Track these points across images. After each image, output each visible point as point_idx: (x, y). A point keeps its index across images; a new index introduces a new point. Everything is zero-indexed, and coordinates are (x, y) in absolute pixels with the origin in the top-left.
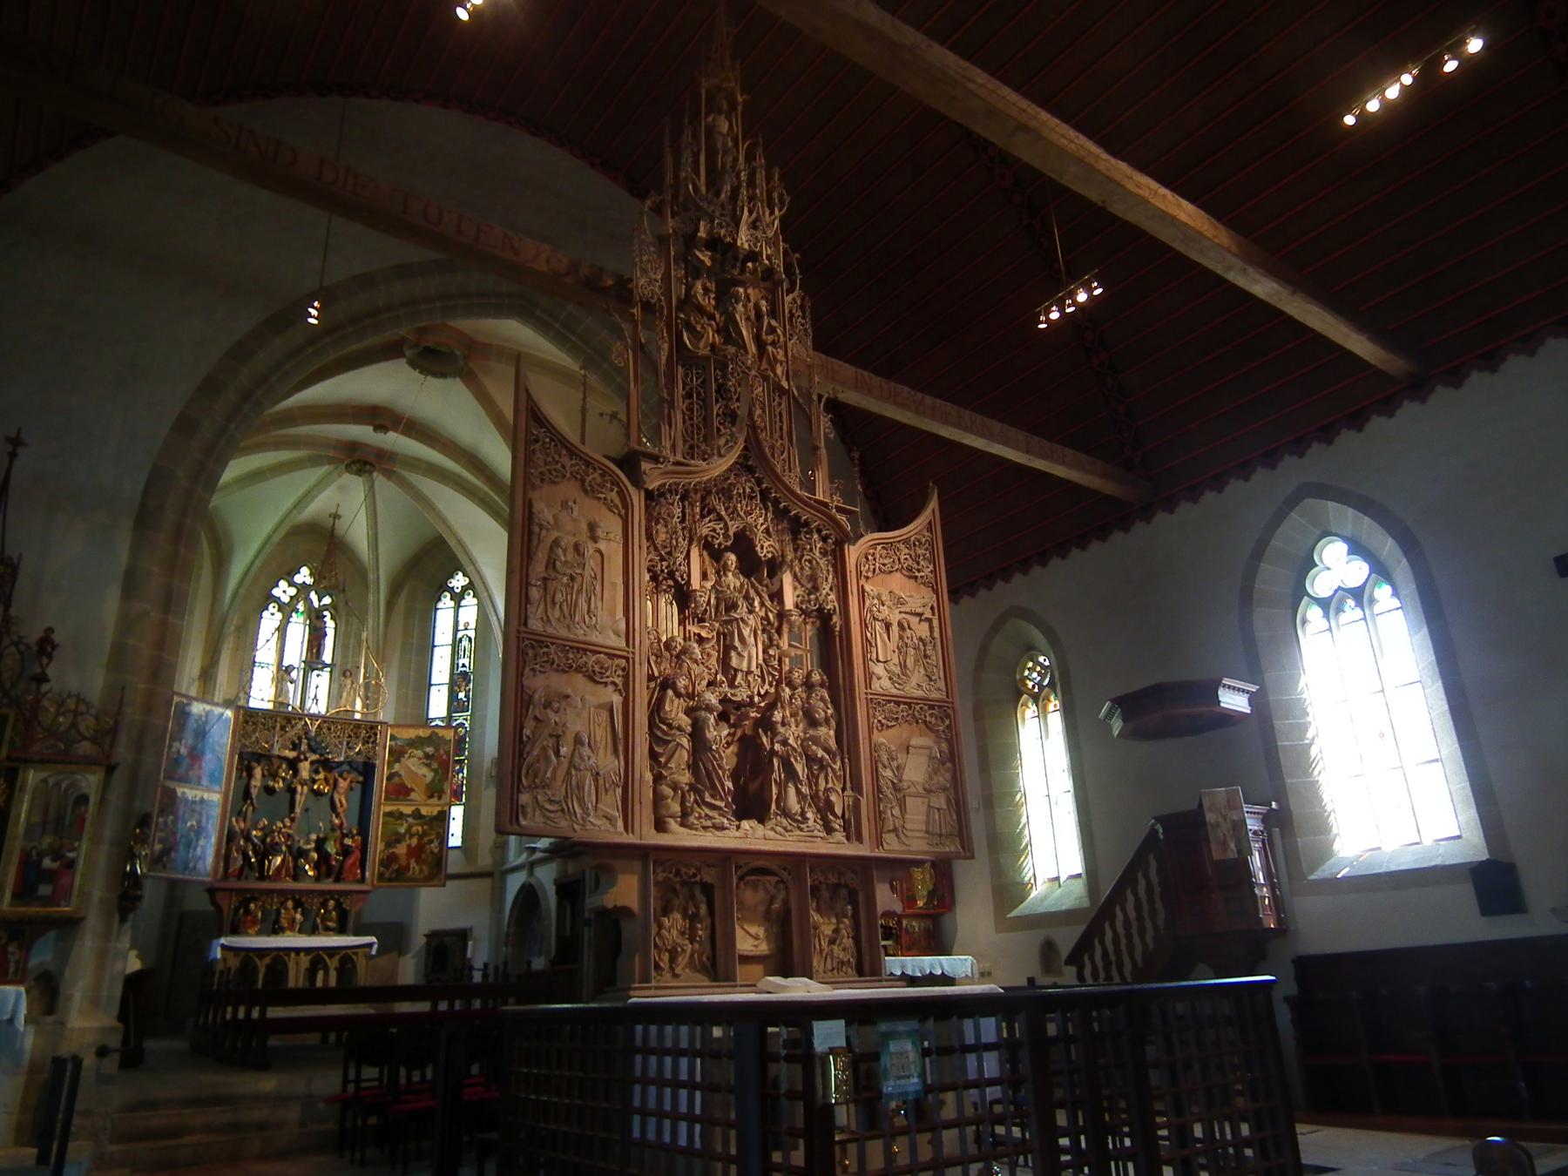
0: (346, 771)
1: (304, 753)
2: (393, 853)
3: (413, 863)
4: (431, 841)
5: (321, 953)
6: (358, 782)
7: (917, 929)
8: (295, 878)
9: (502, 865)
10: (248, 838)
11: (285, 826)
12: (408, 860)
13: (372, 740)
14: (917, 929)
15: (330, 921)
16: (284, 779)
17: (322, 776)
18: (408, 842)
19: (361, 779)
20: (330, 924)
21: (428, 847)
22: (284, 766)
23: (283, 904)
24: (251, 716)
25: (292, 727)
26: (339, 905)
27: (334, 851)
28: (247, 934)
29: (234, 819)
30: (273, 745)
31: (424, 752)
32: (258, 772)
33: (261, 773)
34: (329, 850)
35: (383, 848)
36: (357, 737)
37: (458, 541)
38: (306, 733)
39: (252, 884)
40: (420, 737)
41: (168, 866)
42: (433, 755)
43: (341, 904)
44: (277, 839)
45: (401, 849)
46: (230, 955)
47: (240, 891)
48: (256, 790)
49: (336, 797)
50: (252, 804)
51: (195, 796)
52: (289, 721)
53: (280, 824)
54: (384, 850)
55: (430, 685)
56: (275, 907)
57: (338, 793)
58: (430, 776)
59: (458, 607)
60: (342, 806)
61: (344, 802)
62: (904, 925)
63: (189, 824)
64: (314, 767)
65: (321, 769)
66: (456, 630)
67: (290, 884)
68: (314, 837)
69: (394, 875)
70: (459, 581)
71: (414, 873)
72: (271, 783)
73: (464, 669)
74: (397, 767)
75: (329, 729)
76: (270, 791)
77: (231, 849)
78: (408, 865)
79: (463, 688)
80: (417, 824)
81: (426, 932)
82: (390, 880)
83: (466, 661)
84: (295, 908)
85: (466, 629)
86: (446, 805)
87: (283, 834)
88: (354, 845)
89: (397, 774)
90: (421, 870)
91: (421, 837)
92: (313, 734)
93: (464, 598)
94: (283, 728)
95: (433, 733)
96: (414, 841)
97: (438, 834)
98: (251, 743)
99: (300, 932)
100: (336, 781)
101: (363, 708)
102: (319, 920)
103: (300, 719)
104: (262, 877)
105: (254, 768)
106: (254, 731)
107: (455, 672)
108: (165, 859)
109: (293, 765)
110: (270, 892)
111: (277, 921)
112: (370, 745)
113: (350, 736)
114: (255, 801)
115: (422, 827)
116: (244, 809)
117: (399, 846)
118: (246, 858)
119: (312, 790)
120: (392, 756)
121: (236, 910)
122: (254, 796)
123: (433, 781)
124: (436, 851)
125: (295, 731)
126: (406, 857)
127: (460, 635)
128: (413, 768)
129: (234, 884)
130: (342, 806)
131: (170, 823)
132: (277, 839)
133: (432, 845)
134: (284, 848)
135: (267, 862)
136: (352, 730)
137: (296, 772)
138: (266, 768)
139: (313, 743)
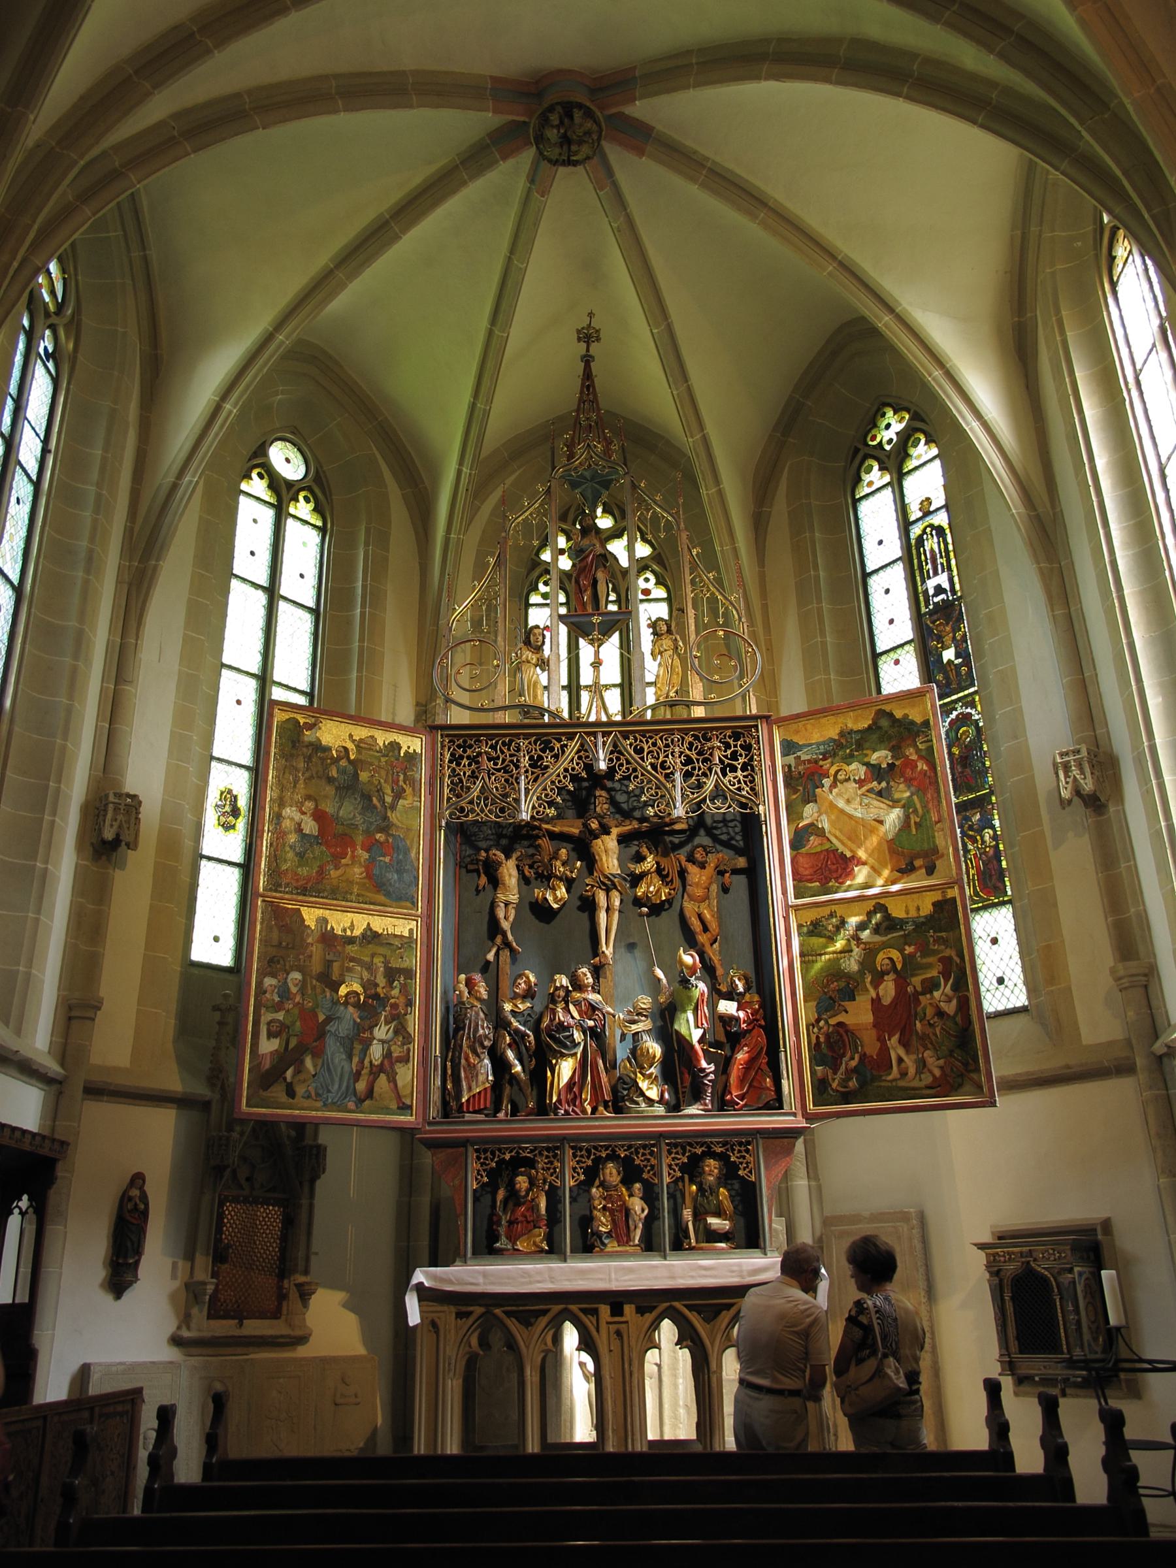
0: (704, 847)
1: (600, 817)
2: (840, 1024)
3: (896, 1050)
4: (931, 986)
5: (677, 1304)
6: (735, 872)
8: (618, 1106)
9: (1157, 1037)
10: (500, 1023)
11: (578, 986)
12: (881, 1040)
13: (741, 760)
15: (718, 1214)
16: (569, 883)
17: (650, 863)
18: (874, 996)
19: (742, 862)
20: (713, 1221)
21: (924, 1000)
23: (592, 1174)
24: (465, 747)
25: (556, 757)
26: (730, 1173)
27: (696, 1034)
28: (516, 1254)
29: (463, 977)
30: (517, 801)
31: (867, 764)
32: (509, 872)
33: (515, 872)
34: (684, 1031)
35: (814, 1016)
36: (705, 760)
37: (841, 264)
38: (589, 768)
40: (851, 732)
41: (300, 1090)
42: (891, 766)
43: (734, 1167)
44: (561, 1015)
45: (859, 1014)
46: (447, 1315)
47: (486, 1146)
48: (512, 914)
49: (689, 907)
50: (507, 944)
51: (352, 927)
52: (547, 747)
54: (818, 1021)
55: (876, 656)
56: (570, 1182)
57: (691, 898)
58: (893, 817)
59: (899, 477)
60: (706, 929)
61: (707, 915)
63: (343, 990)
64: (634, 849)
65: (644, 851)
66: (905, 525)
67: (609, 1123)
68: (645, 1002)
69: (853, 1084)
70: (891, 428)
71: (904, 1074)
72: (538, 893)
73: (943, 596)
74: (809, 812)
75: (639, 751)
76: (542, 911)
77: (461, 1046)
78: (884, 1051)
79: (948, 639)
80: (885, 946)
81: (987, 1238)
82: (846, 1098)
83: (942, 580)
84: (627, 1181)
85: (927, 513)
86: (950, 885)
87: (577, 1004)
88: (741, 1014)
89: (813, 829)
90: (922, 1065)
91: (902, 980)
92: (603, 766)
93: (908, 456)
94: (535, 763)
95: (881, 713)
96: (888, 990)
97: (946, 961)
98: (471, 802)
99: (650, 1245)
100: (682, 873)
101: (707, 690)
102: (687, 1214)
103: (571, 737)
104: (543, 1109)
105: (500, 864)
106: (474, 776)
107: (924, 610)
108: (289, 1074)
109: (583, 849)
110: (554, 1146)
111: (585, 1222)
112: (739, 773)
113: (689, 761)
114: (510, 937)
115: (901, 951)
116: (490, 956)
117: (846, 1004)
118: (501, 1066)
119: (638, 902)
120: (796, 791)
122: (506, 925)
123: (906, 824)
124: (950, 1008)
125: (564, 763)
126: (873, 1033)
127: (916, 531)
128: (848, 809)
129: (475, 1126)
130: (706, 929)
131: (294, 990)
132: (561, 1015)
133: (937, 994)
134: (578, 1036)
135: (549, 1074)
136: (691, 744)
137: (591, 862)
138: (529, 862)
139: (621, 798)
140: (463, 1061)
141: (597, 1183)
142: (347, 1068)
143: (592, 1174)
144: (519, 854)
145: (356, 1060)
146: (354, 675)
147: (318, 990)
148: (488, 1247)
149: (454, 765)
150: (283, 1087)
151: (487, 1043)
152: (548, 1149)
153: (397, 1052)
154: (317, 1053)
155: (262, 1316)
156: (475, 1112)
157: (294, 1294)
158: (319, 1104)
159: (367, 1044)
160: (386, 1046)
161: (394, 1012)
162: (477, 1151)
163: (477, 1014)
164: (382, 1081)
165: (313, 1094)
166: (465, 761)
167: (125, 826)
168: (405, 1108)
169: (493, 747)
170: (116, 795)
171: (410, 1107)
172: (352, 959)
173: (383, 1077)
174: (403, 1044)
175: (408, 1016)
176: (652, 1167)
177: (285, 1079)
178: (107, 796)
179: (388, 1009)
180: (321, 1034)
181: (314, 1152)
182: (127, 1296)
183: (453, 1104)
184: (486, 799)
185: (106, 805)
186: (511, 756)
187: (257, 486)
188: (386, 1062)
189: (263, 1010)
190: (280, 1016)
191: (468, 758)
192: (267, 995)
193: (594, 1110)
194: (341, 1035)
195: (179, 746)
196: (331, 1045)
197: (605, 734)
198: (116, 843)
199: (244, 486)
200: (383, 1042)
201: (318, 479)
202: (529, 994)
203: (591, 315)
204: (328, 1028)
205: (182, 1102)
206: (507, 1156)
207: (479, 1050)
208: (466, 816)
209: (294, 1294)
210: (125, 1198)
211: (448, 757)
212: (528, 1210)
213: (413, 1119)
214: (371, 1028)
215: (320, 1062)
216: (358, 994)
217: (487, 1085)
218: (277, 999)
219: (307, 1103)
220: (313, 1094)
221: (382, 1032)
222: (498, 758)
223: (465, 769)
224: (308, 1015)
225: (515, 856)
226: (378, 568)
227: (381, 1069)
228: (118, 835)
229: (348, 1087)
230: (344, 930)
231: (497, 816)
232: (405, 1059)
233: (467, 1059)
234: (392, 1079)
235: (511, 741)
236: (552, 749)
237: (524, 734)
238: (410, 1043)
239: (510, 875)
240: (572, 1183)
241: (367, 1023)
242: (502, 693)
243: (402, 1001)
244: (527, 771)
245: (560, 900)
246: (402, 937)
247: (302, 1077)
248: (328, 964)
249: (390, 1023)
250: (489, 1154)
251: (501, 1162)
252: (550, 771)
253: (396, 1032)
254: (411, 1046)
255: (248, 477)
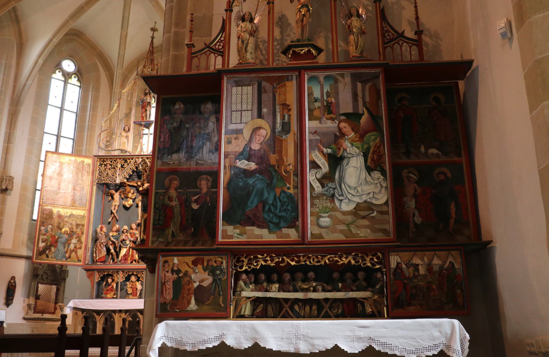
7: (422, 271)
14: (422, 271)
22: (132, 191)
23: (128, 279)
24: (104, 161)
28: (106, 298)
29: (100, 226)
30: (116, 177)
32: (117, 196)
39: (110, 265)
41: (50, 256)
47: (99, 271)
50: (115, 217)
52: (126, 161)
53: (126, 227)
62: (393, 265)
63: (63, 230)
87: (131, 234)
94: (122, 166)
103: (132, 159)
105: (114, 194)
108: (47, 252)
110: (117, 271)
114: (116, 215)
118: (108, 250)
121: (99, 284)
122: (114, 211)
129: (100, 266)
131: (49, 230)
140: (97, 249)
141: (130, 281)
142: (63, 250)
143: (128, 279)
144: (120, 191)
145: (66, 248)
146: (86, 133)
147: (56, 230)
148: (99, 296)
149: (100, 167)
150: (45, 255)
151: (104, 244)
152: (116, 272)
153: (78, 246)
154: (55, 247)
155: (50, 313)
156: (101, 262)
157: (59, 308)
158: (55, 259)
159: (69, 244)
160: (75, 245)
161: (78, 236)
162: (98, 272)
163: (103, 236)
164: (73, 253)
165: (54, 257)
166: (103, 166)
167: (8, 185)
168: (80, 261)
169: (111, 162)
170: (6, 176)
171: (81, 261)
172: (66, 222)
173: (74, 253)
174: (80, 244)
175: (82, 237)
176: (142, 277)
177: (46, 253)
178: (3, 176)
179: (76, 235)
180: (56, 242)
181: (65, 271)
182: (10, 307)
183: (95, 260)
184: (108, 176)
185: (3, 179)
186: (116, 164)
187: (58, 75)
188: (75, 249)
189: (41, 235)
190: (45, 237)
191: (104, 164)
192: (42, 232)
193: (132, 262)
194: (62, 242)
195: (28, 160)
196: (59, 244)
197: (142, 158)
198: (6, 189)
199: (54, 76)
200: (74, 244)
201: (78, 71)
202: (118, 231)
203: (156, 23)
204: (59, 240)
205: (27, 258)
206: (106, 274)
207: (102, 246)
208: (102, 181)
209: (59, 308)
210: (10, 282)
211: (99, 164)
212: (111, 287)
213: (81, 264)
214: (71, 240)
215: (56, 249)
216: (67, 231)
217: (104, 255)
218: (44, 232)
219: (52, 259)
220: (54, 257)
221: (74, 241)
222: (112, 165)
223: (103, 168)
224: (53, 237)
225: (119, 191)
226: (95, 100)
227: (73, 251)
228: (7, 187)
229: (63, 255)
230: (64, 214)
231: (111, 181)
232: (80, 248)
233: (99, 248)
234: (76, 253)
235: (116, 160)
236: (127, 162)
237: (119, 158)
238: (82, 244)
239: (117, 197)
240: (122, 281)
241: (70, 239)
242: (116, 145)
243: (80, 233)
244: (120, 169)
245: (130, 204)
246: (81, 215)
247: (50, 252)
248: (59, 223)
249: (77, 238)
250: (101, 273)
251: (104, 275)
252: (126, 169)
253: (78, 241)
254: (82, 245)
255: (55, 72)
